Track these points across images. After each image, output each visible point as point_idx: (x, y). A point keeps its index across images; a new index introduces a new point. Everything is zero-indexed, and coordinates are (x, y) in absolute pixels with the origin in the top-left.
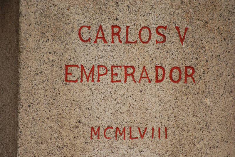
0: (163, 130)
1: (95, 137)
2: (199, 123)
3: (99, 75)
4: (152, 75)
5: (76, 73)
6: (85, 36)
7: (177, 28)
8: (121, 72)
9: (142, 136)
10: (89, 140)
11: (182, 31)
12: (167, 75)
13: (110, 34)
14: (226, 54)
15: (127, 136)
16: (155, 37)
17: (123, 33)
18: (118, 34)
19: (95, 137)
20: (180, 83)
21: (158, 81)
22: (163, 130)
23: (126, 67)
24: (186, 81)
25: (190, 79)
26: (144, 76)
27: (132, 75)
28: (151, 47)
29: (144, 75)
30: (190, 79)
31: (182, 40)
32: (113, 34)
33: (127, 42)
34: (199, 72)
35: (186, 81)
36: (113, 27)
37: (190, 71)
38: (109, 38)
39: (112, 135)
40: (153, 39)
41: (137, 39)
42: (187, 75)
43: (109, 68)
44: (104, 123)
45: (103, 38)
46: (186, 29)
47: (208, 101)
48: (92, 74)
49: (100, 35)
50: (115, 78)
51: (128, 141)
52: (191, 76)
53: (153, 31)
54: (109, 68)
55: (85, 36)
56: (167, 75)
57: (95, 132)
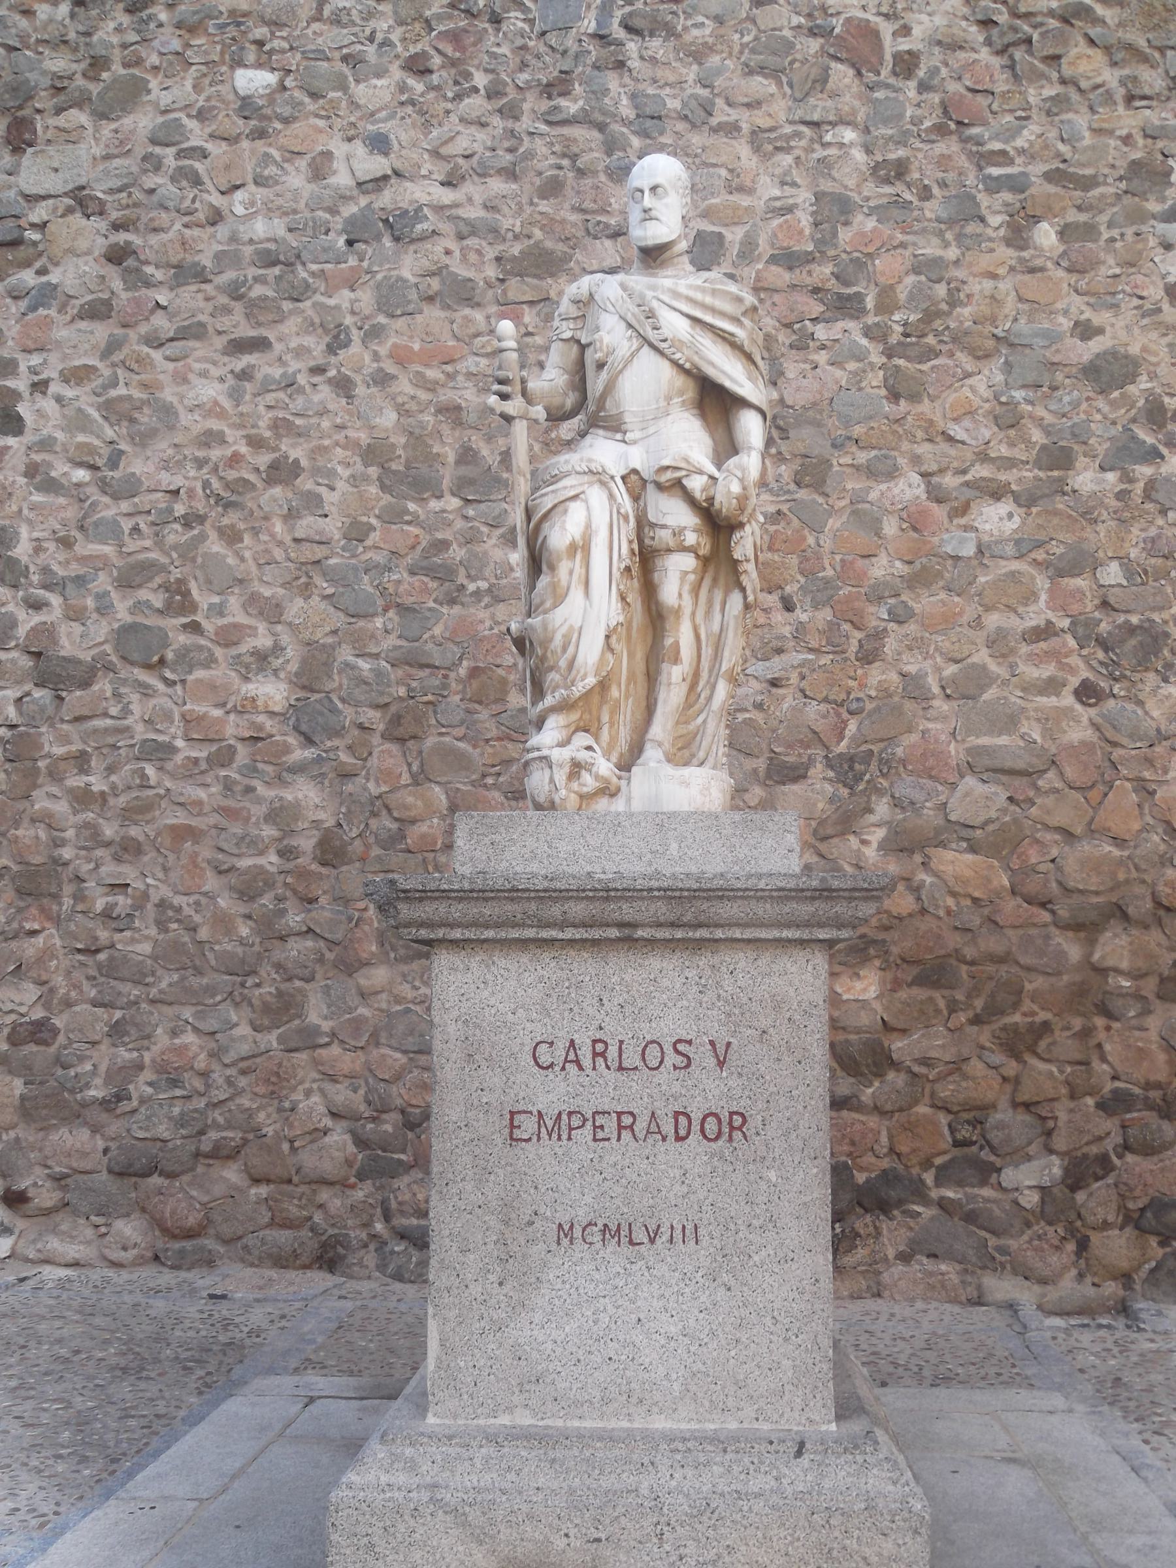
0: (690, 1227)
1: (565, 1242)
3: (571, 1129)
4: (668, 1128)
5: (528, 1125)
6: (545, 1060)
7: (712, 1043)
8: (611, 1124)
9: (652, 1241)
10: (554, 1247)
11: (721, 1050)
12: (696, 1127)
13: (589, 1056)
15: (624, 1240)
16: (671, 1058)
17: (612, 1052)
18: (603, 1054)
19: (565, 1242)
20: (720, 1143)
21: (679, 1138)
22: (690, 1227)
23: (619, 1114)
24: (731, 1139)
25: (737, 1135)
26: (654, 1129)
27: (631, 1127)
28: (663, 1076)
29: (654, 1128)
30: (737, 1135)
31: (721, 1064)
32: (595, 1054)
33: (621, 1068)
34: (754, 1123)
35: (731, 1139)
36: (595, 1042)
37: (738, 1121)
38: (587, 1062)
39: (597, 1238)
40: (668, 1062)
41: (638, 1063)
42: (732, 1128)
43: (589, 1115)
44: (582, 1215)
45: (577, 1062)
46: (729, 1044)
48: (559, 1126)
49: (572, 1057)
50: (600, 1135)
51: (626, 1249)
52: (740, 1128)
53: (669, 1050)
54: (589, 1115)
55: (545, 1060)
56: (696, 1127)
57: (565, 1232)
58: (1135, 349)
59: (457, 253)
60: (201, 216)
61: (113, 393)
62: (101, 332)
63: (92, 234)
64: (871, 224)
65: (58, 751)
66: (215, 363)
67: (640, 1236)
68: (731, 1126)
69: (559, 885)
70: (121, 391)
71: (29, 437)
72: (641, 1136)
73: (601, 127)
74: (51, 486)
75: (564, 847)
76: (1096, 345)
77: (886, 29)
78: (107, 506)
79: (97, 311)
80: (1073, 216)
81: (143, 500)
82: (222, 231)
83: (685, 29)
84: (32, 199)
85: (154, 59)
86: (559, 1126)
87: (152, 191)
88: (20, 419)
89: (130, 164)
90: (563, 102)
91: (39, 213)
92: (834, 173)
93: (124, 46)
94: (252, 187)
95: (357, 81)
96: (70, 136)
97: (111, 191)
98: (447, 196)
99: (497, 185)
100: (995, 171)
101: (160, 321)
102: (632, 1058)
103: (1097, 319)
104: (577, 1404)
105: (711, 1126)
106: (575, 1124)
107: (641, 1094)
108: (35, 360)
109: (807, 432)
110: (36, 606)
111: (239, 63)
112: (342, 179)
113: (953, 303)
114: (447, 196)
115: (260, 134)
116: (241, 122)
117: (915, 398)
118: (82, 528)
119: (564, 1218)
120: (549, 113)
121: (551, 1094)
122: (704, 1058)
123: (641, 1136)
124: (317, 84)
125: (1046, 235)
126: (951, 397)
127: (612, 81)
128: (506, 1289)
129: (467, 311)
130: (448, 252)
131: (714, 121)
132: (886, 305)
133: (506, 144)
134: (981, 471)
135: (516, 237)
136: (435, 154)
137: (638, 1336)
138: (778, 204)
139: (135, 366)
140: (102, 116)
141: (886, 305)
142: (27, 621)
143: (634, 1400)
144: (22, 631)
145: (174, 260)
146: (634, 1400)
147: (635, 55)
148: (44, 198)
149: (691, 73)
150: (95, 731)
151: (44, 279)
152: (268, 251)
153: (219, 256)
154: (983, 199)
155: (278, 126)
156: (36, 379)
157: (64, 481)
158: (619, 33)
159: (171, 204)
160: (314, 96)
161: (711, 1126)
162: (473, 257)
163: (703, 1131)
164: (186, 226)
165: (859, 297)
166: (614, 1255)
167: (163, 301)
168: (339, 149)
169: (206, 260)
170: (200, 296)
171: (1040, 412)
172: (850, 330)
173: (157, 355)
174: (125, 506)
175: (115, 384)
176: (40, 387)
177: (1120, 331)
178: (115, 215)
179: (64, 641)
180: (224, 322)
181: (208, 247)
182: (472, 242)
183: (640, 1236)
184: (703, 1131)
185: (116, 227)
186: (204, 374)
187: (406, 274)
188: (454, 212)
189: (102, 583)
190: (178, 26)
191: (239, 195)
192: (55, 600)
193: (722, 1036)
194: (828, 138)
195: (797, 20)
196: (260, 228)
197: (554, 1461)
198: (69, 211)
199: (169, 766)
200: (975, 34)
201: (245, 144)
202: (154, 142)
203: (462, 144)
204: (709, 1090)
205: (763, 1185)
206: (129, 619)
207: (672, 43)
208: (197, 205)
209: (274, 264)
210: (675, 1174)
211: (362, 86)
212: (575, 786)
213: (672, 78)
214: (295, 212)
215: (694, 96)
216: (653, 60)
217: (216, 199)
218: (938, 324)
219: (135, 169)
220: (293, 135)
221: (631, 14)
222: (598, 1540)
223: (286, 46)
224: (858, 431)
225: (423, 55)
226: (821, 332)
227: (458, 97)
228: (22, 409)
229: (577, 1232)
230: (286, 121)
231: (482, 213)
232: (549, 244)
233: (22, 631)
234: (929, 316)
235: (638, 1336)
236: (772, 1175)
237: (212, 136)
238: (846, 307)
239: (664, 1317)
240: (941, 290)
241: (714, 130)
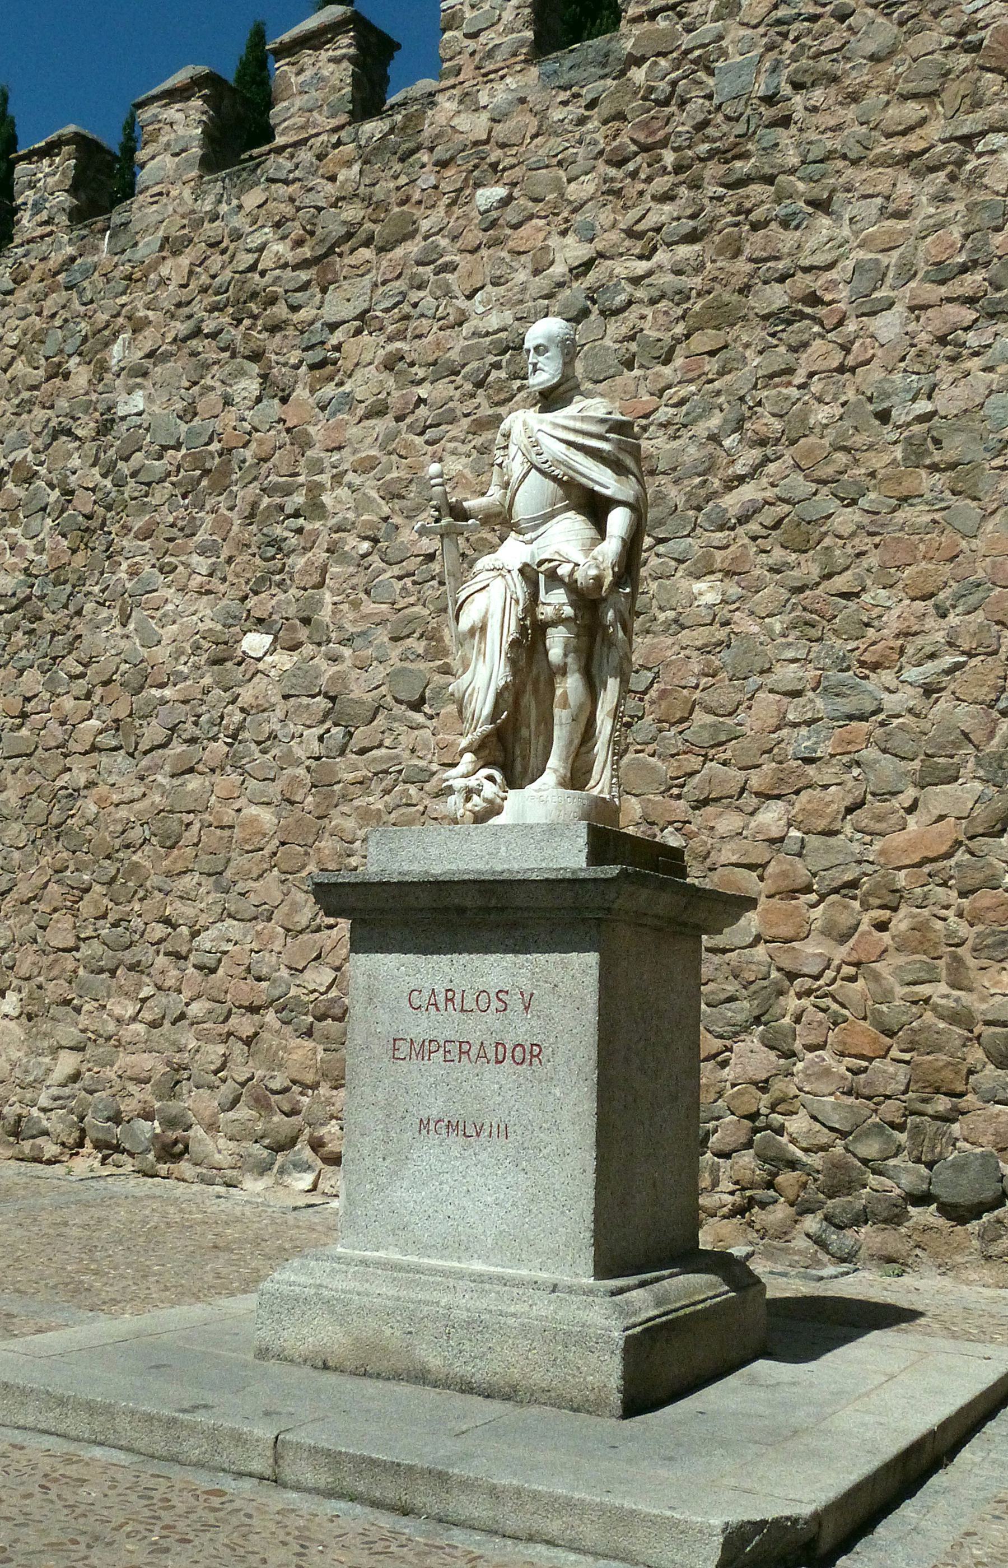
0: (502, 1127)
1: (424, 1132)
2: (546, 1122)
3: (430, 1052)
4: (491, 1055)
5: (404, 1048)
6: (416, 1003)
7: (522, 993)
8: (454, 1048)
9: (478, 1135)
10: (417, 1135)
11: (527, 997)
12: (509, 1054)
13: (443, 999)
14: (579, 1028)
15: (461, 1133)
16: (495, 1004)
17: (458, 999)
18: (452, 1000)
19: (424, 1132)
20: (524, 1066)
21: (498, 1062)
22: (502, 1127)
23: (461, 1043)
24: (531, 1064)
25: (536, 1061)
26: (482, 1055)
27: (467, 1052)
28: (490, 1017)
29: (482, 1054)
30: (536, 1061)
31: (527, 1008)
32: (447, 1000)
33: (462, 1010)
34: (547, 1052)
35: (531, 1064)
36: (447, 990)
37: (536, 1049)
38: (442, 1006)
39: (444, 1131)
40: (493, 1007)
41: (474, 1006)
42: (532, 1056)
43: (442, 1043)
44: (434, 1113)
45: (436, 1005)
46: (532, 995)
47: (557, 1091)
48: (423, 1049)
49: (432, 1001)
50: (449, 1057)
51: (461, 1139)
52: (537, 1056)
53: (493, 995)
54: (442, 1043)
55: (416, 1003)
56: (509, 1054)
57: (423, 1124)
59: (650, 318)
60: (451, 318)
61: (388, 477)
62: (381, 425)
63: (371, 347)
65: (350, 777)
66: (463, 442)
67: (470, 1131)
68: (529, 1054)
69: (407, 878)
70: (395, 474)
71: (331, 522)
72: (473, 1059)
73: (769, 180)
74: (344, 559)
75: (433, 851)
78: (385, 571)
79: (378, 411)
81: (410, 565)
82: (466, 329)
83: (845, 72)
84: (333, 327)
85: (417, 196)
86: (423, 1049)
87: (415, 305)
88: (323, 506)
89: (401, 285)
90: (738, 164)
91: (338, 336)
92: (986, 181)
93: (398, 189)
94: (489, 288)
95: (569, 181)
96: (361, 270)
97: (387, 310)
98: (642, 267)
99: (684, 251)
101: (422, 411)
102: (470, 1004)
104: (425, 1247)
105: (519, 1052)
106: (433, 1049)
107: (476, 1029)
108: (336, 457)
109: (959, 438)
110: (334, 659)
111: (478, 185)
112: (559, 270)
114: (642, 267)
115: (496, 243)
116: (481, 234)
118: (367, 592)
119: (424, 1114)
120: (724, 176)
121: (421, 1027)
122: (515, 1003)
123: (473, 1059)
124: (538, 191)
127: (784, 136)
128: (387, 1163)
129: (659, 368)
130: (643, 317)
131: (871, 156)
133: (689, 212)
135: (699, 295)
136: (630, 233)
137: (466, 1202)
138: (931, 221)
139: (403, 453)
140: (381, 250)
142: (329, 670)
143: (463, 1248)
144: (323, 680)
145: (431, 359)
146: (463, 1248)
147: (800, 107)
148: (345, 322)
149: (850, 113)
150: (374, 760)
151: (341, 389)
152: (501, 340)
153: (464, 350)
155: (508, 231)
156: (335, 471)
157: (353, 553)
158: (786, 90)
159: (430, 313)
160: (536, 200)
161: (519, 1052)
162: (662, 319)
163: (513, 1057)
164: (440, 329)
166: (455, 1142)
167: (424, 396)
168: (554, 241)
169: (454, 355)
170: (452, 386)
173: (419, 440)
174: (396, 570)
175: (389, 470)
176: (337, 479)
178: (390, 329)
179: (353, 686)
180: (469, 405)
181: (457, 344)
182: (662, 305)
183: (470, 1131)
184: (513, 1057)
185: (390, 339)
186: (453, 453)
187: (608, 342)
188: (647, 281)
189: (382, 635)
190: (436, 164)
191: (478, 296)
192: (347, 652)
193: (527, 988)
194: (979, 148)
195: (947, 40)
196: (493, 321)
197: (395, 1279)
198: (358, 332)
199: (427, 787)
201: (484, 252)
202: (419, 263)
203: (652, 220)
204: (520, 1029)
205: (551, 1098)
206: (399, 664)
207: (833, 89)
208: (450, 310)
209: (504, 352)
210: (497, 1085)
211: (573, 185)
212: (469, 805)
213: (832, 123)
214: (521, 302)
215: (853, 135)
216: (815, 109)
217: (462, 303)
219: (403, 288)
220: (519, 239)
221: (796, 71)
222: (410, 1333)
223: (514, 161)
225: (622, 147)
226: (972, 339)
227: (649, 180)
228: (326, 499)
229: (432, 1127)
230: (516, 227)
231: (670, 277)
232: (726, 297)
233: (323, 680)
235: (466, 1202)
236: (557, 1091)
237: (461, 251)
239: (484, 1190)
241: (872, 164)
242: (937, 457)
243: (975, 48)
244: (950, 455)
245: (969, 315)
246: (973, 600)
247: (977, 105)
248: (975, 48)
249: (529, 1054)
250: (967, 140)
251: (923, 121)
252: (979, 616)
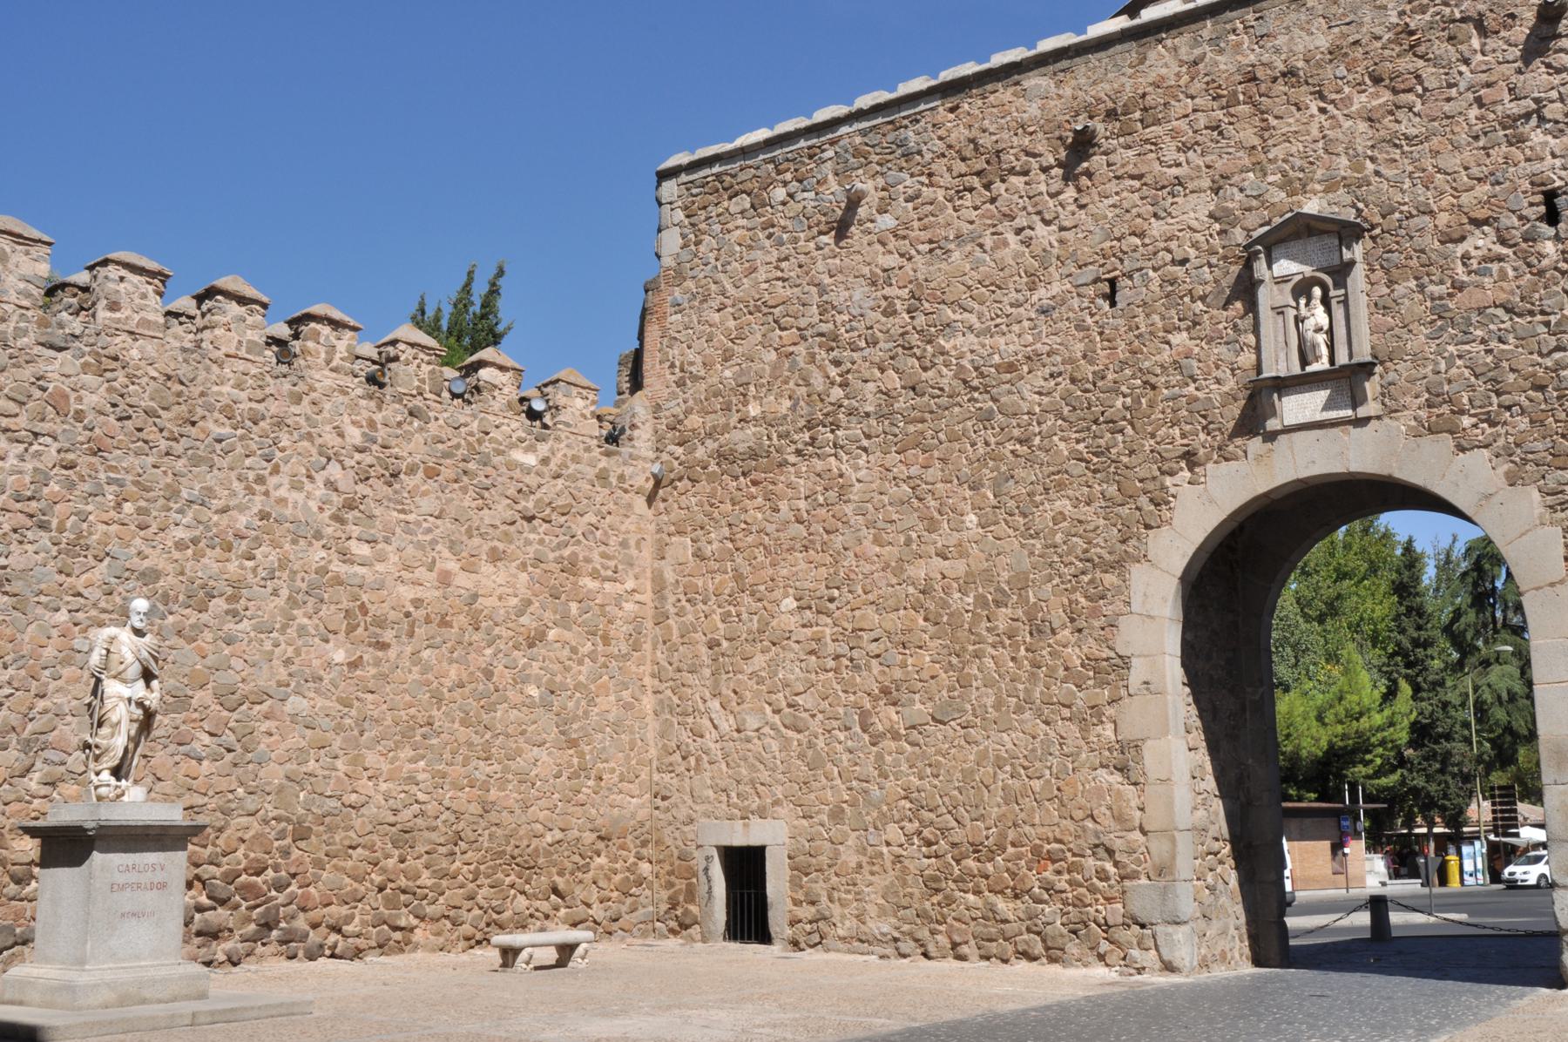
48: (122, 888)
58: (160, 567)
64: (57, 488)
68: (162, 886)
76: (146, 563)
77: (73, 395)
80: (142, 503)
86: (122, 888)
100: (112, 475)
103: (148, 551)
109: (20, 583)
113: (91, 534)
117: (68, 575)
121: (121, 879)
125: (128, 507)
126: (84, 577)
132: (61, 530)
134: (93, 613)
141: (61, 530)
154: (106, 487)
165: (49, 522)
166: (134, 921)
171: (120, 589)
172: (45, 539)
177: (155, 560)
200: (109, 409)
218: (82, 542)
224: (43, 586)
226: (29, 534)
234: (80, 536)
238: (43, 526)
240: (85, 525)
242: (8, 588)
243: (44, 390)
244: (16, 590)
245: (29, 523)
246: (20, 663)
247: (43, 420)
248: (44, 390)
249: (162, 886)
250: (36, 435)
251: (16, 415)
252: (23, 672)
